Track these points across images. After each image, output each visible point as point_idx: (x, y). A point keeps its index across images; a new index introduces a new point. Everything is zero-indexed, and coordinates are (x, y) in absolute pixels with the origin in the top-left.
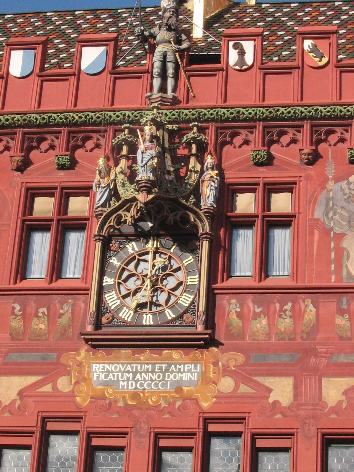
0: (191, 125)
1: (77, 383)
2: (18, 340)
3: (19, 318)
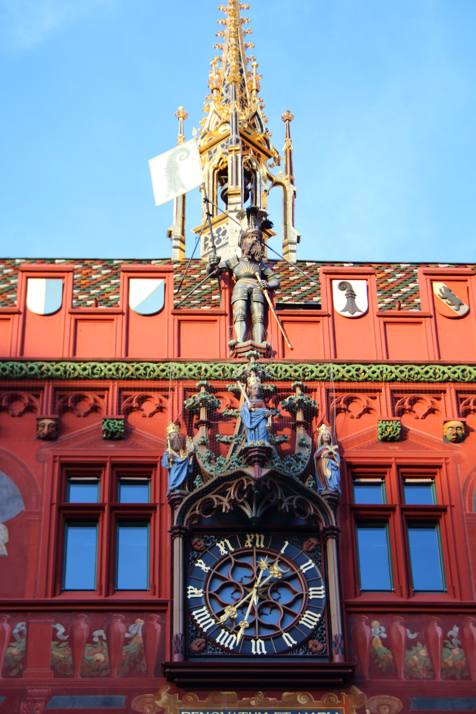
0: (293, 384)
2: (65, 676)
3: (64, 644)
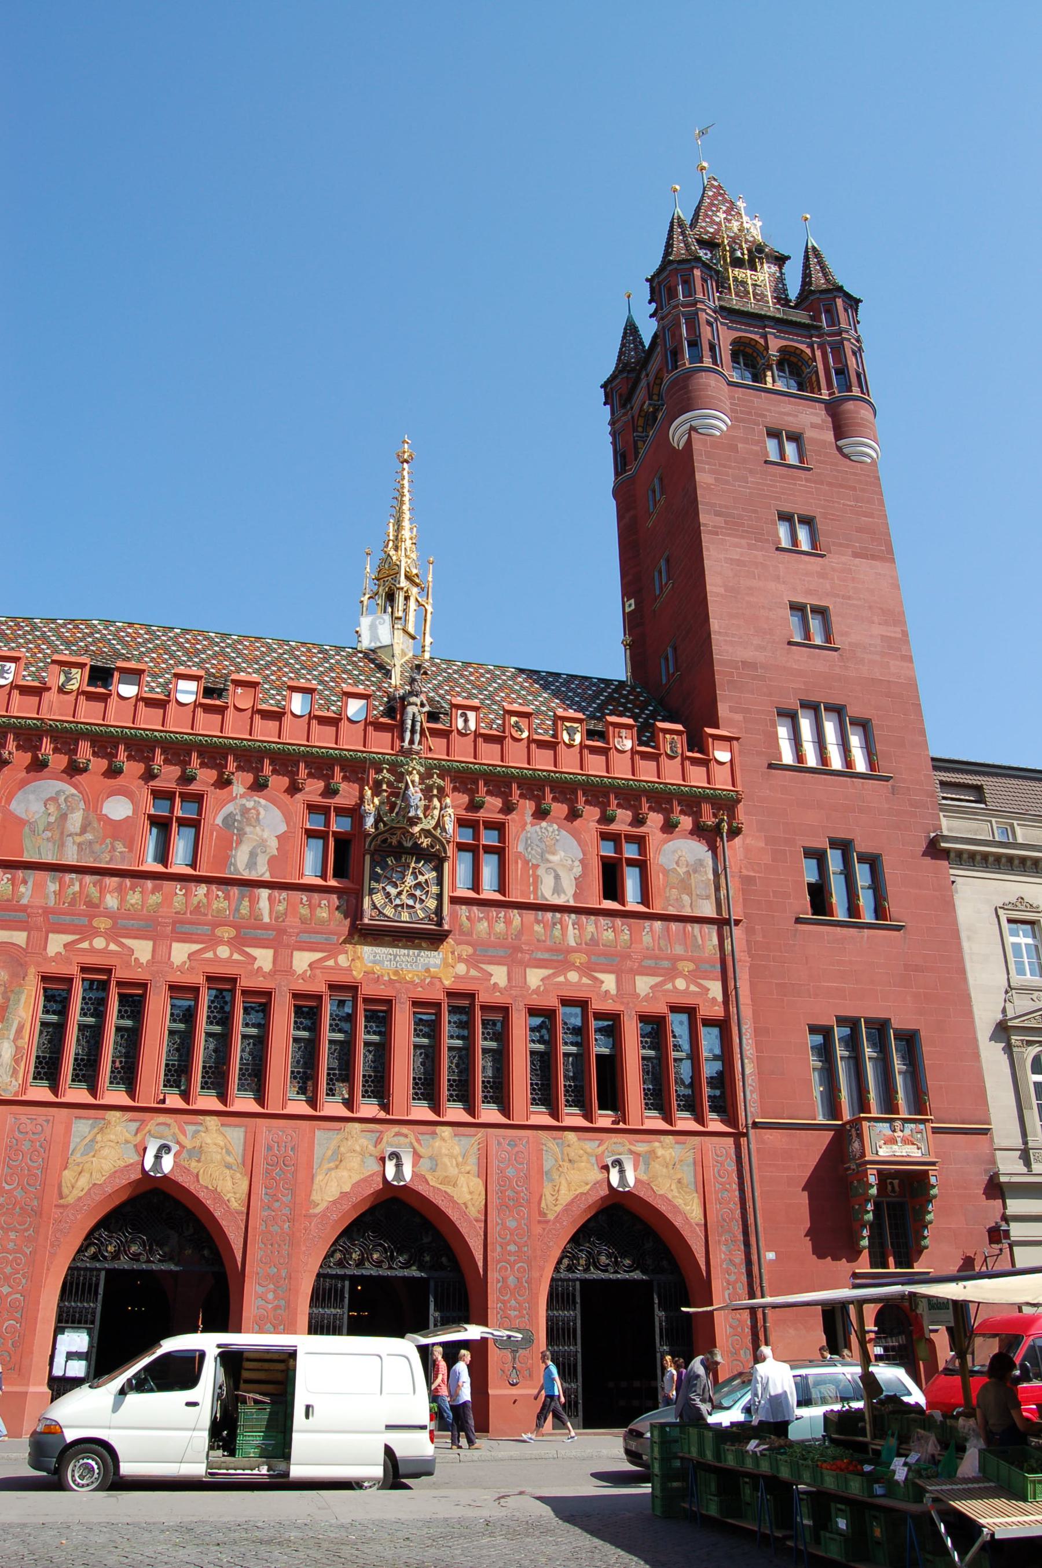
1: (353, 960)
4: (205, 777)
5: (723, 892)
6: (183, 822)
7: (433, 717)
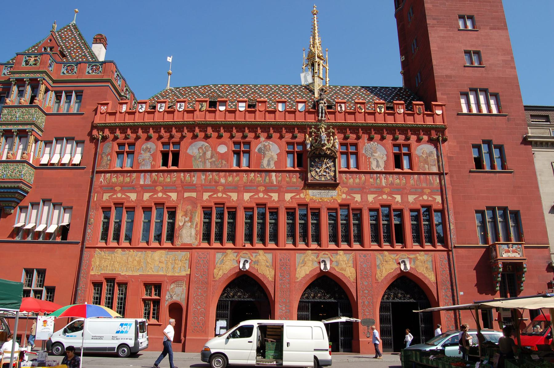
4: (251, 135)
5: (440, 163)
6: (244, 152)
7: (329, 107)
